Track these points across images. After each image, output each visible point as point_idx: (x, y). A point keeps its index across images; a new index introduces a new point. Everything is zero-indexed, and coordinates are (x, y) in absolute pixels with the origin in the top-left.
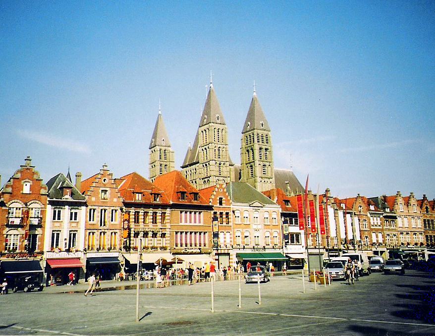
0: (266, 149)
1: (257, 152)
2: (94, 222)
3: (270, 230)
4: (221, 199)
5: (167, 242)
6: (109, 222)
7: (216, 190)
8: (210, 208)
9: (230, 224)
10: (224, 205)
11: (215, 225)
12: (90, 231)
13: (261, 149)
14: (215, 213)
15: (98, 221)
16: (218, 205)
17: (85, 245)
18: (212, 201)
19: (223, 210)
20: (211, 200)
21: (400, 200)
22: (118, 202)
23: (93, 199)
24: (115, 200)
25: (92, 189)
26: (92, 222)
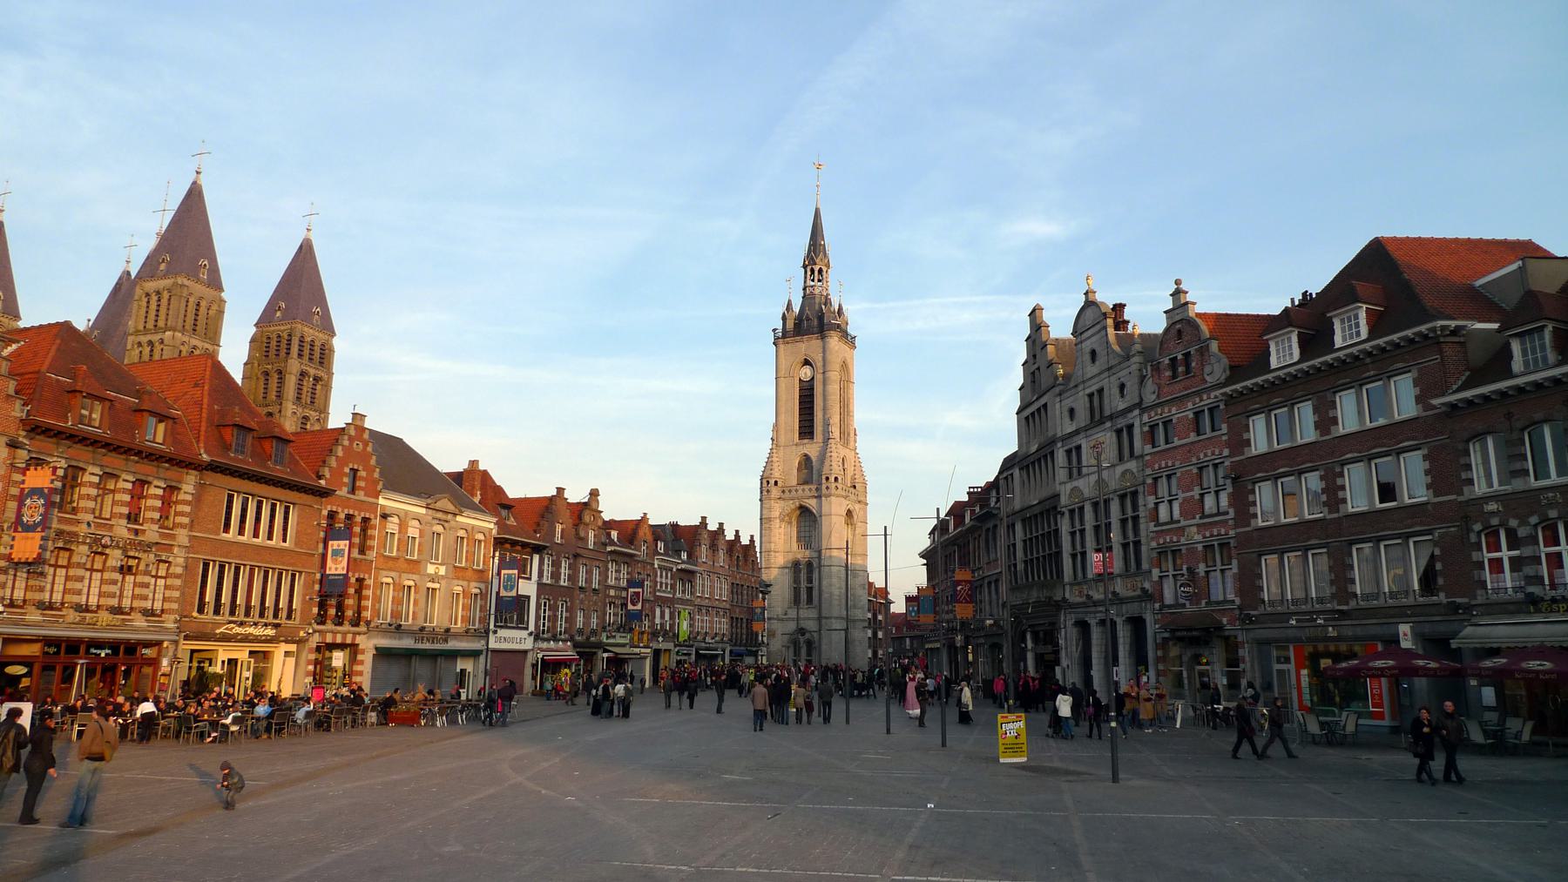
0: (317, 379)
1: (291, 382)
3: (465, 583)
4: (354, 471)
5: (168, 594)
7: (346, 443)
8: (324, 493)
9: (372, 555)
10: (360, 495)
11: (337, 553)
13: (303, 374)
14: (332, 516)
16: (343, 492)
18: (328, 476)
19: (355, 509)
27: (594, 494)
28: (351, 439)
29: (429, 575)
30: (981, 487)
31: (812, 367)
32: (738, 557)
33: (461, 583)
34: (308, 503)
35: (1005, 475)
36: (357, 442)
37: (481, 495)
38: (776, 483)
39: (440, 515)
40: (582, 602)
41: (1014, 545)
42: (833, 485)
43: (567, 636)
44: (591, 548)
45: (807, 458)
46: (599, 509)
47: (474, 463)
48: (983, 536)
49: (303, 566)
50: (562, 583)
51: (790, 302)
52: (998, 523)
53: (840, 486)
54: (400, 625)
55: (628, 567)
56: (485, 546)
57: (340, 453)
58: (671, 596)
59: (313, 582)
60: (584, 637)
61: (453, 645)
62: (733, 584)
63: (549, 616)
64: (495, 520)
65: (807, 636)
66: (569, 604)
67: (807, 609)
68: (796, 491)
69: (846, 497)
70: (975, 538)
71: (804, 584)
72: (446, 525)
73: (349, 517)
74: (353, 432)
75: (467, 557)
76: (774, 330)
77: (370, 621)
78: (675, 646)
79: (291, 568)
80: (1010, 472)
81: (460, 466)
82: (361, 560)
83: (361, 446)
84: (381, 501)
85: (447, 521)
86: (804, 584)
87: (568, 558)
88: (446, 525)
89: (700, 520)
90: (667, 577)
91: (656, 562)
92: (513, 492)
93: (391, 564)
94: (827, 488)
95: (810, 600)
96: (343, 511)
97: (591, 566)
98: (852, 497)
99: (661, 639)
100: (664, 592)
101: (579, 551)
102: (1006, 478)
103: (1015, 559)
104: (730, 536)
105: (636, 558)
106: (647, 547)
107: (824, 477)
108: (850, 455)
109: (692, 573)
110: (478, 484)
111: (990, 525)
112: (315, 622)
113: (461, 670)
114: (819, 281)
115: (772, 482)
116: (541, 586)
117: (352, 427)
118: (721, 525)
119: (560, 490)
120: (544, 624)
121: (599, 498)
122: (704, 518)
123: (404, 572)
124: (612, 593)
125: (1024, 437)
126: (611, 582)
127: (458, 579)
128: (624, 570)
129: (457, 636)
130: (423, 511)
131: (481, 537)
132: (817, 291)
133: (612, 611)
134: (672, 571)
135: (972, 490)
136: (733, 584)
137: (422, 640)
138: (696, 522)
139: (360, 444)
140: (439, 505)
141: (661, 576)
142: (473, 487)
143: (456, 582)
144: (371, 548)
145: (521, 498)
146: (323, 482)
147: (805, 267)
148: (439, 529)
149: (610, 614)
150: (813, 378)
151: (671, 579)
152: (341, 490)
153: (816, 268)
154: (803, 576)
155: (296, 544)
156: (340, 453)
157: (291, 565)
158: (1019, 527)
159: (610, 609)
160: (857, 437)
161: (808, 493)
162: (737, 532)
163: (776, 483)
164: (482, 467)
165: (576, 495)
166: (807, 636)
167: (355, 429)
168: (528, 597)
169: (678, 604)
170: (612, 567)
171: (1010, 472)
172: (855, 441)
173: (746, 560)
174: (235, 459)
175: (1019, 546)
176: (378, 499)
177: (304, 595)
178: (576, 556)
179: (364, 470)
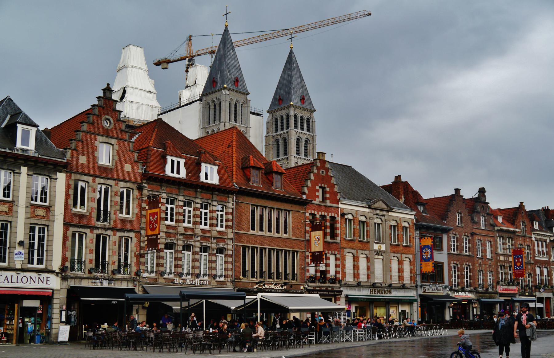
2: (84, 211)
3: (399, 255)
6: (115, 214)
7: (315, 171)
9: (338, 239)
10: (328, 203)
12: (76, 229)
15: (92, 209)
17: (64, 259)
18: (307, 192)
19: (325, 211)
20: (306, 190)
22: (134, 171)
23: (83, 160)
24: (128, 167)
25: (80, 136)
26: (78, 209)
27: (482, 191)
28: (318, 169)
29: (375, 251)
33: (396, 255)
34: (297, 210)
36: (321, 170)
37: (404, 197)
39: (378, 212)
40: (480, 265)
43: (472, 288)
44: (484, 228)
46: (487, 201)
47: (398, 178)
49: (298, 248)
50: (465, 253)
54: (360, 283)
56: (410, 231)
57: (312, 177)
58: (547, 260)
59: (305, 257)
60: (485, 289)
61: (395, 294)
63: (458, 275)
64: (414, 213)
66: (459, 266)
72: (383, 218)
73: (323, 217)
74: (319, 164)
75: (398, 238)
77: (341, 280)
79: (291, 249)
81: (389, 181)
82: (332, 243)
83: (325, 172)
84: (340, 206)
85: (382, 216)
87: (467, 236)
88: (383, 218)
90: (542, 247)
92: (426, 195)
93: (350, 244)
96: (318, 213)
97: (485, 240)
99: (542, 290)
101: (474, 231)
106: (525, 226)
110: (401, 191)
112: (309, 281)
113: (402, 311)
116: (449, 255)
117: (318, 161)
119: (457, 191)
120: (455, 280)
121: (485, 194)
123: (359, 249)
124: (502, 258)
126: (500, 251)
127: (394, 252)
128: (509, 244)
129: (396, 288)
130: (367, 210)
131: (406, 225)
133: (503, 271)
134: (545, 241)
137: (375, 291)
139: (324, 171)
140: (377, 205)
141: (538, 246)
142: (399, 193)
143: (393, 255)
144: (337, 235)
145: (432, 199)
146: (304, 196)
148: (379, 221)
149: (502, 273)
151: (546, 248)
152: (315, 200)
155: (293, 235)
156: (312, 177)
157: (291, 247)
159: (501, 270)
164: (403, 180)
165: (469, 193)
167: (320, 162)
168: (442, 263)
170: (500, 241)
174: (253, 187)
176: (339, 204)
177: (301, 265)
178: (473, 234)
179: (327, 187)
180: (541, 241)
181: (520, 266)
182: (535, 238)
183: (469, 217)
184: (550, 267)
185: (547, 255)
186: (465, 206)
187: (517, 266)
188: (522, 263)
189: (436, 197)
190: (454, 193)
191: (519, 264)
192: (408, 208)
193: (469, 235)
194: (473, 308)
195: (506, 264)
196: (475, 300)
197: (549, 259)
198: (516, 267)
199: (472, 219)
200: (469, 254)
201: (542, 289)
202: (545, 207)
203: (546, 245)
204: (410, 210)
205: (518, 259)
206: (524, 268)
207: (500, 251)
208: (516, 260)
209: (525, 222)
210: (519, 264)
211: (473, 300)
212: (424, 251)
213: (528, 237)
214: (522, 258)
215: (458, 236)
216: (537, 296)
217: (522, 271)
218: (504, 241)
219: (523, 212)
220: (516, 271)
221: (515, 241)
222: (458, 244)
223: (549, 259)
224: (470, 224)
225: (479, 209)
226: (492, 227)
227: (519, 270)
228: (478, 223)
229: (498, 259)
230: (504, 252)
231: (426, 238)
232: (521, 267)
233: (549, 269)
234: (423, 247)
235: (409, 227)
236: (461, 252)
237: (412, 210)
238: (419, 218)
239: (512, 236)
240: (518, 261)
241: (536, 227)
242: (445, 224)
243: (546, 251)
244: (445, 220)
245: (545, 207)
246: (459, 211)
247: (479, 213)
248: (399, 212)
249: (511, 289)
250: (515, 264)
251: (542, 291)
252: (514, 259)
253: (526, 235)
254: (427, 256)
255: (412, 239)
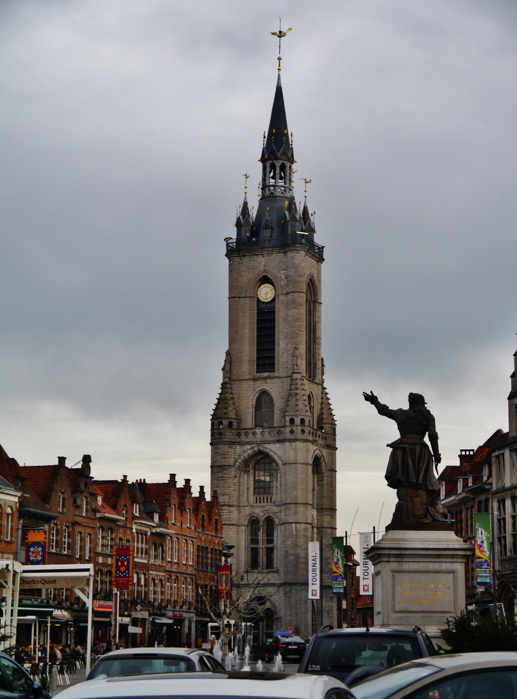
21: (174, 500)
27: (87, 459)
30: (473, 450)
31: (273, 285)
32: (203, 516)
35: (497, 453)
38: (230, 424)
41: (504, 519)
42: (299, 429)
45: (264, 393)
48: (476, 506)
51: (245, 204)
52: (490, 497)
53: (307, 430)
55: (112, 533)
58: (146, 562)
60: (80, 605)
62: (198, 546)
64: (19, 494)
65: (268, 605)
67: (267, 573)
68: (254, 433)
69: (313, 442)
70: (468, 508)
71: (262, 545)
76: (226, 240)
78: (150, 615)
80: (502, 452)
86: (262, 545)
89: (168, 478)
90: (142, 543)
91: (134, 527)
94: (292, 432)
95: (270, 564)
98: (320, 441)
99: (139, 607)
100: (140, 558)
102: (498, 457)
103: (505, 532)
104: (180, 484)
105: (118, 523)
106: (127, 511)
107: (288, 419)
108: (316, 390)
109: (163, 536)
111: (483, 498)
114: (281, 178)
115: (225, 422)
118: (188, 481)
122: (173, 476)
125: (514, 414)
126: (99, 549)
131: (9, 511)
132: (278, 192)
134: (146, 535)
135: (463, 453)
136: (198, 546)
138: (165, 479)
141: (138, 542)
147: (263, 160)
150: (274, 300)
151: (146, 544)
153: (278, 164)
154: (261, 536)
158: (508, 503)
160: (325, 369)
161: (268, 437)
162: (188, 481)
163: (230, 424)
166: (268, 605)
169: (152, 570)
171: (502, 452)
172: (323, 374)
173: (210, 520)
175: (509, 521)
178: (75, 524)
180: (142, 534)
181: (125, 572)
182: (136, 529)
183: (72, 498)
184: (148, 573)
185: (146, 554)
186: (68, 483)
187: (120, 572)
188: (127, 568)
189: (27, 465)
190: (56, 462)
191: (123, 569)
192: (10, 487)
193: (70, 525)
194: (67, 633)
195: (104, 568)
196: (71, 621)
197: (148, 561)
198: (119, 574)
199: (75, 502)
200: (68, 552)
201: (139, 606)
202: (141, 480)
203: (146, 539)
204: (13, 489)
205: (123, 562)
206: (130, 575)
207: (99, 549)
208: (126, 563)
209: (127, 505)
210: (123, 569)
211: (70, 621)
212: (32, 549)
213: (129, 528)
214: (128, 560)
215: (59, 527)
216: (132, 617)
217: (127, 579)
218: (104, 534)
219: (126, 491)
220: (118, 579)
221: (115, 534)
222: (70, 541)
223: (148, 561)
224: (72, 509)
225: (82, 487)
226: (93, 513)
227: (122, 577)
228: (78, 507)
229: (97, 561)
230: (102, 550)
231: (36, 531)
232: (126, 574)
233: (147, 577)
234: (30, 543)
235: (12, 514)
236: (61, 551)
237: (16, 489)
238: (22, 502)
239: (112, 525)
240: (123, 565)
241: (136, 513)
242: (48, 510)
243: (146, 549)
244: (48, 503)
245: (141, 480)
246: (63, 491)
247: (82, 492)
248: (6, 492)
249: (107, 606)
250: (118, 568)
251: (139, 609)
252: (117, 561)
253: (126, 524)
254: (36, 557)
255: (14, 532)
